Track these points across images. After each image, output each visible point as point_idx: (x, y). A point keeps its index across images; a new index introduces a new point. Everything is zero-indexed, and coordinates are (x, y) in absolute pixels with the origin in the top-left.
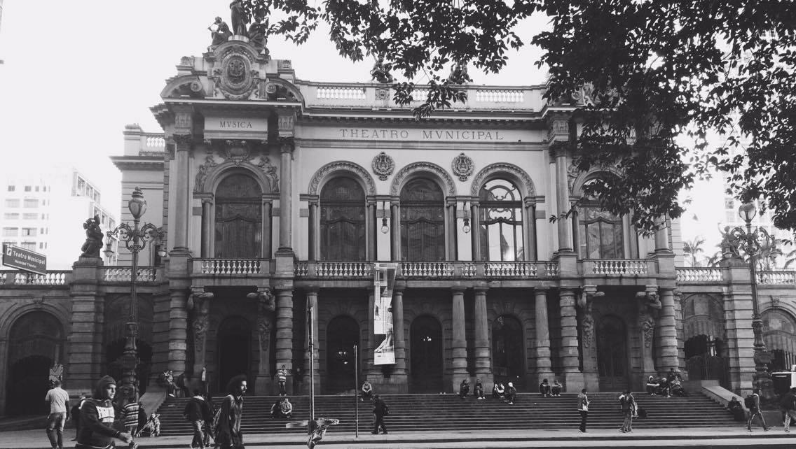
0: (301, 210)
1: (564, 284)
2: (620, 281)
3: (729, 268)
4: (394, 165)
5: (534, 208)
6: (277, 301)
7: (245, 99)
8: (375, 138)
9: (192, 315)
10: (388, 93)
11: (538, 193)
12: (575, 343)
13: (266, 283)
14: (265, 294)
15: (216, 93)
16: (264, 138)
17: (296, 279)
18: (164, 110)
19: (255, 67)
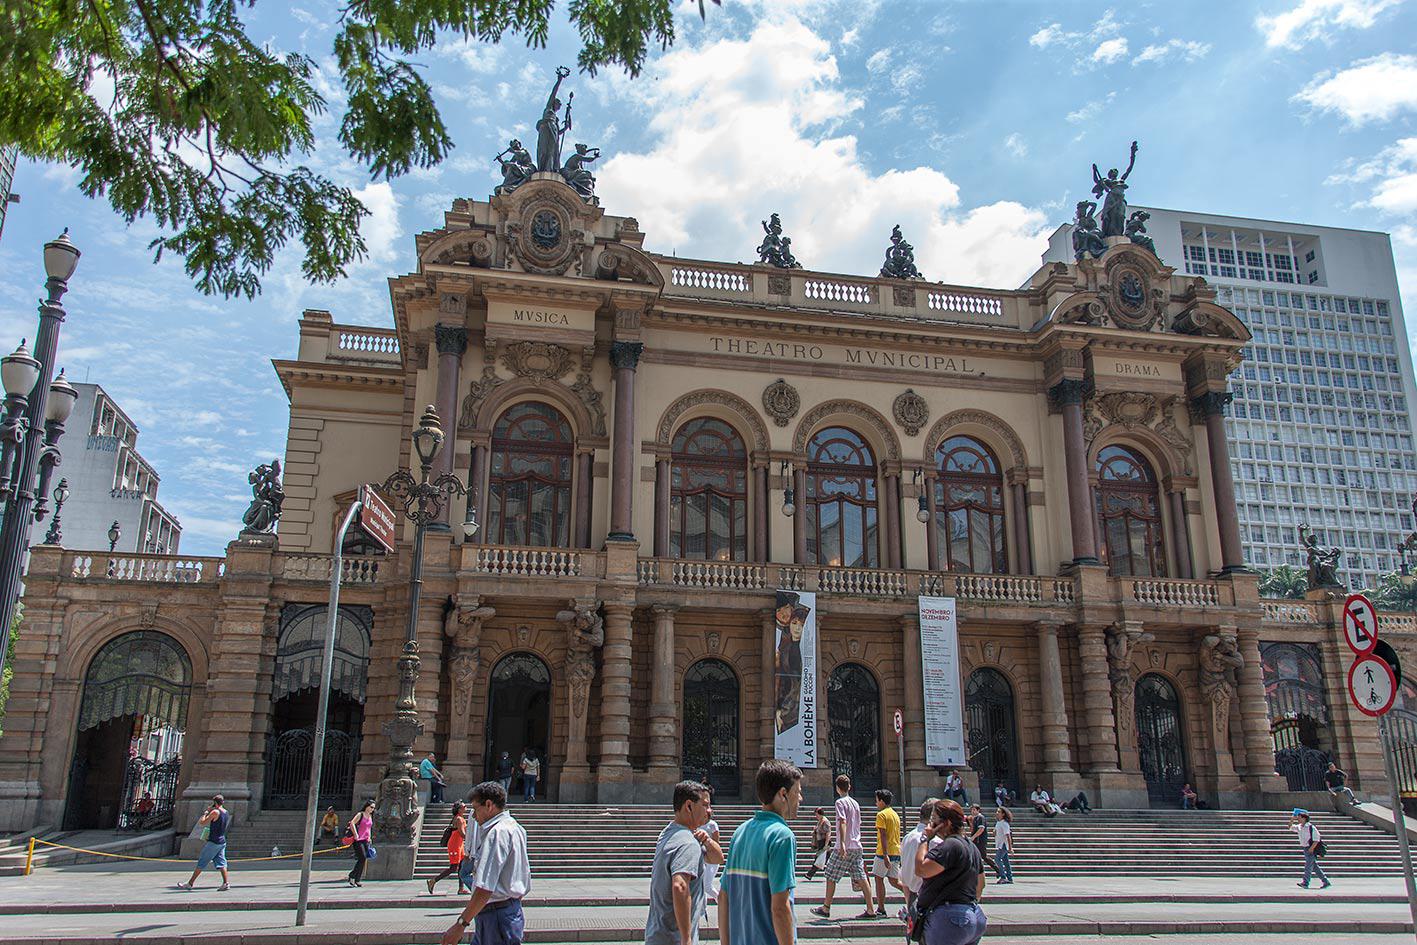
6: (605, 627)
8: (768, 355)
12: (1109, 720)
13: (590, 593)
18: (417, 285)
19: (576, 224)
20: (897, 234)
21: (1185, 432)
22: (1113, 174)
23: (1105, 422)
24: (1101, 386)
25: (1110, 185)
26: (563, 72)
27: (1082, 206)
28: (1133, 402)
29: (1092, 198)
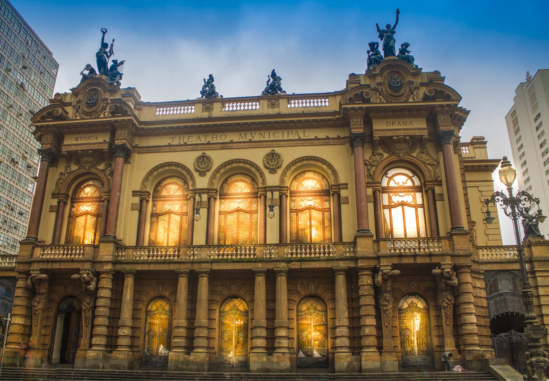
0: (132, 204)
1: (360, 264)
2: (415, 260)
4: (212, 163)
6: (97, 283)
7: (98, 118)
8: (198, 142)
9: (32, 292)
10: (212, 106)
11: (342, 180)
14: (85, 275)
15: (76, 117)
16: (106, 147)
17: (115, 263)
20: (273, 74)
21: (434, 156)
22: (388, 26)
23: (386, 155)
26: (105, 31)
29: (378, 40)
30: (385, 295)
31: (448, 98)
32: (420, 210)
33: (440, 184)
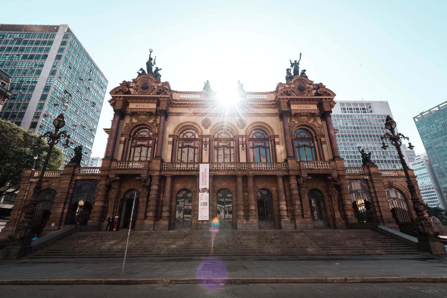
1: (291, 173)
3: (368, 167)
5: (274, 140)
11: (276, 133)
17: (160, 171)
19: (154, 84)
22: (296, 61)
24: (293, 112)
25: (295, 65)
27: (288, 70)
28: (303, 116)
29: (291, 68)
30: (303, 189)
31: (329, 95)
32: (313, 149)
33: (324, 136)
